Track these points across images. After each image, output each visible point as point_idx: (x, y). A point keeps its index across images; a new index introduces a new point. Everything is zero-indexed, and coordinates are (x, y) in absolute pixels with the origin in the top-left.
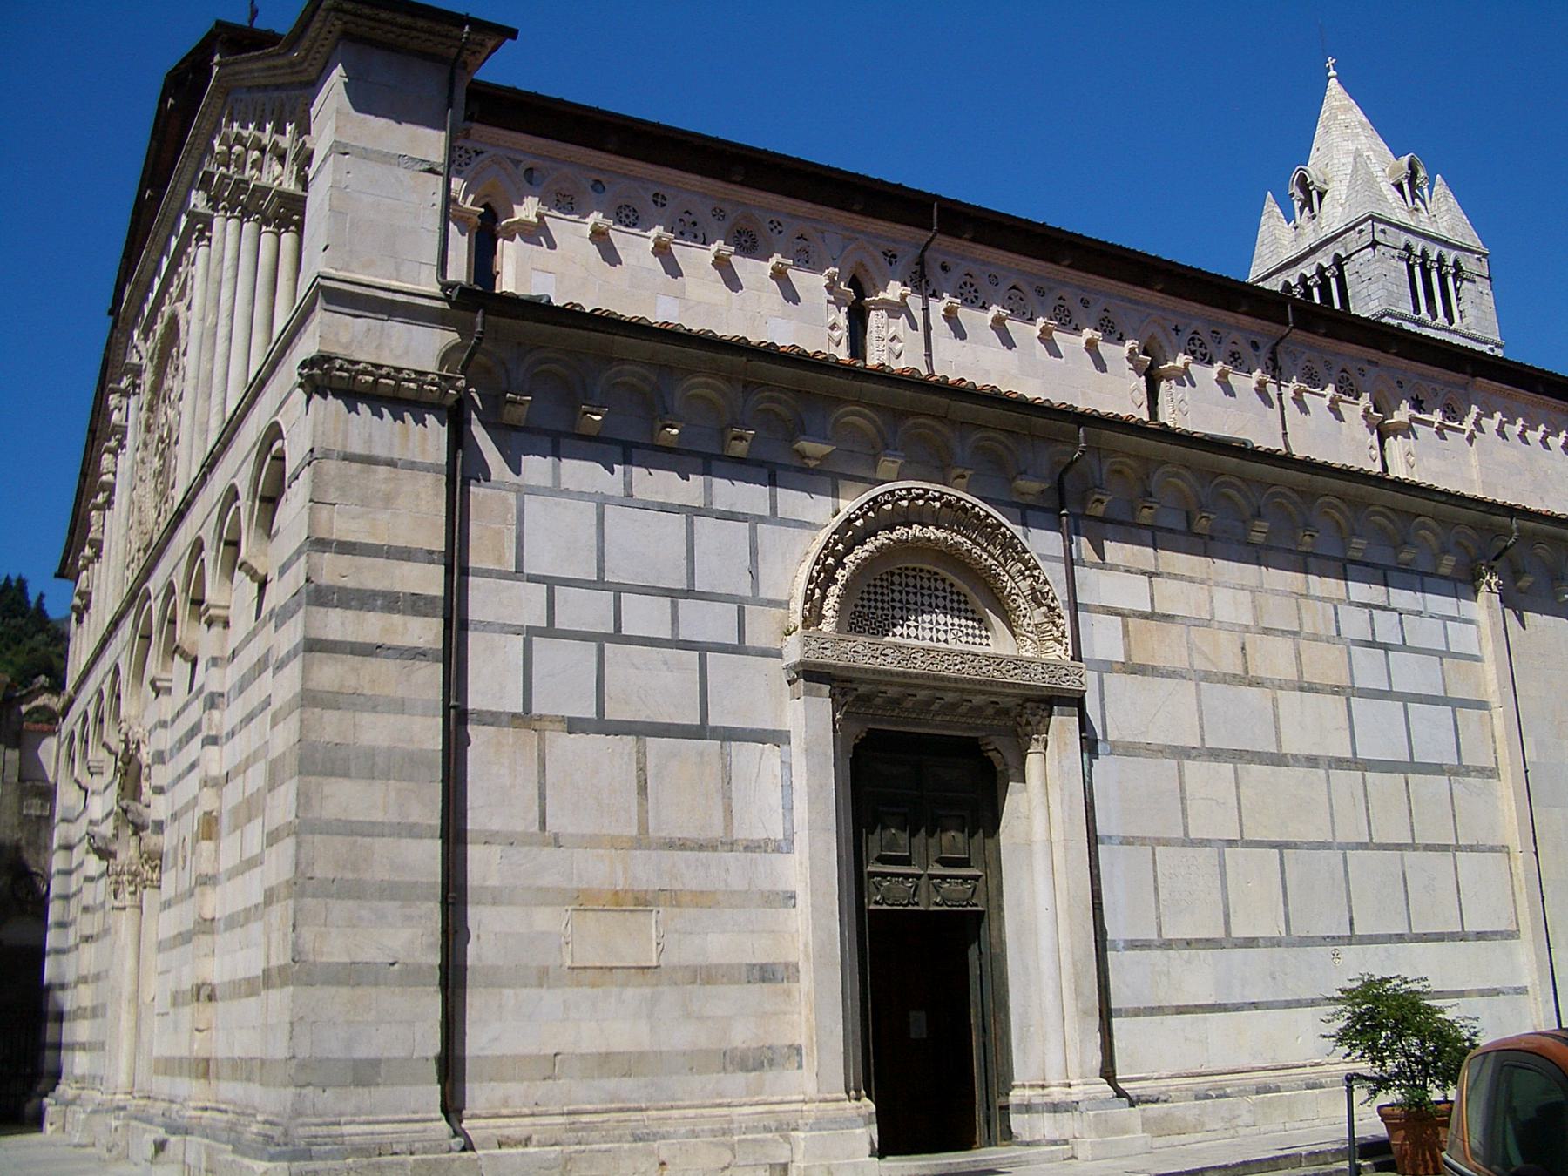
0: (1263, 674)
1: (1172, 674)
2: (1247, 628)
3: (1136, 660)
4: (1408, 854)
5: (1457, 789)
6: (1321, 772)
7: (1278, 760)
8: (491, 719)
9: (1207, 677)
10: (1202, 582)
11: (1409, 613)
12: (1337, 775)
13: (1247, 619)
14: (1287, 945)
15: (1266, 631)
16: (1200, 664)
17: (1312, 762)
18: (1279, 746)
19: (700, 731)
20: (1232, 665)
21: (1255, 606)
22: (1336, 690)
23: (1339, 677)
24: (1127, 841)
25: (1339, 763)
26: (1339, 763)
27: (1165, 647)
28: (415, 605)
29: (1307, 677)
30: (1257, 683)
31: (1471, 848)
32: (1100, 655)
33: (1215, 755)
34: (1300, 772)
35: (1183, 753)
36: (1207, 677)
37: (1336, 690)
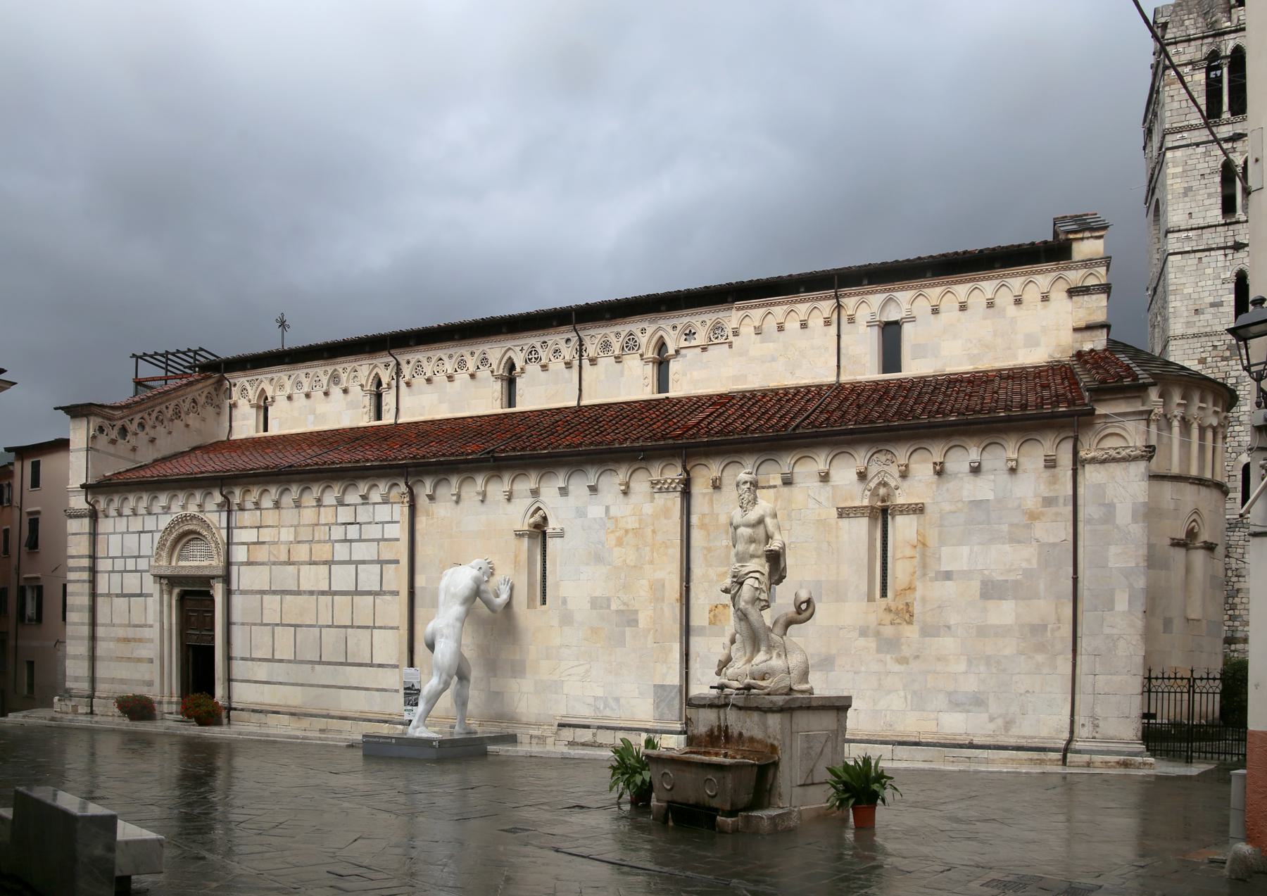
0: (295, 560)
1: (263, 564)
2: (291, 542)
3: (251, 560)
4: (350, 630)
5: (377, 601)
6: (315, 597)
7: (298, 593)
8: (102, 595)
9: (274, 563)
10: (277, 527)
11: (365, 523)
12: (322, 598)
13: (292, 539)
14: (296, 663)
15: (299, 542)
16: (272, 559)
17: (311, 593)
18: (299, 587)
19: (140, 595)
20: (284, 558)
21: (296, 532)
22: (325, 563)
23: (328, 557)
24: (243, 624)
25: (323, 593)
26: (323, 593)
27: (262, 554)
28: (81, 569)
29: (313, 559)
30: (293, 564)
31: (380, 628)
32: (240, 560)
33: (274, 592)
34: (306, 597)
35: (263, 592)
36: (274, 563)
37: (325, 563)
